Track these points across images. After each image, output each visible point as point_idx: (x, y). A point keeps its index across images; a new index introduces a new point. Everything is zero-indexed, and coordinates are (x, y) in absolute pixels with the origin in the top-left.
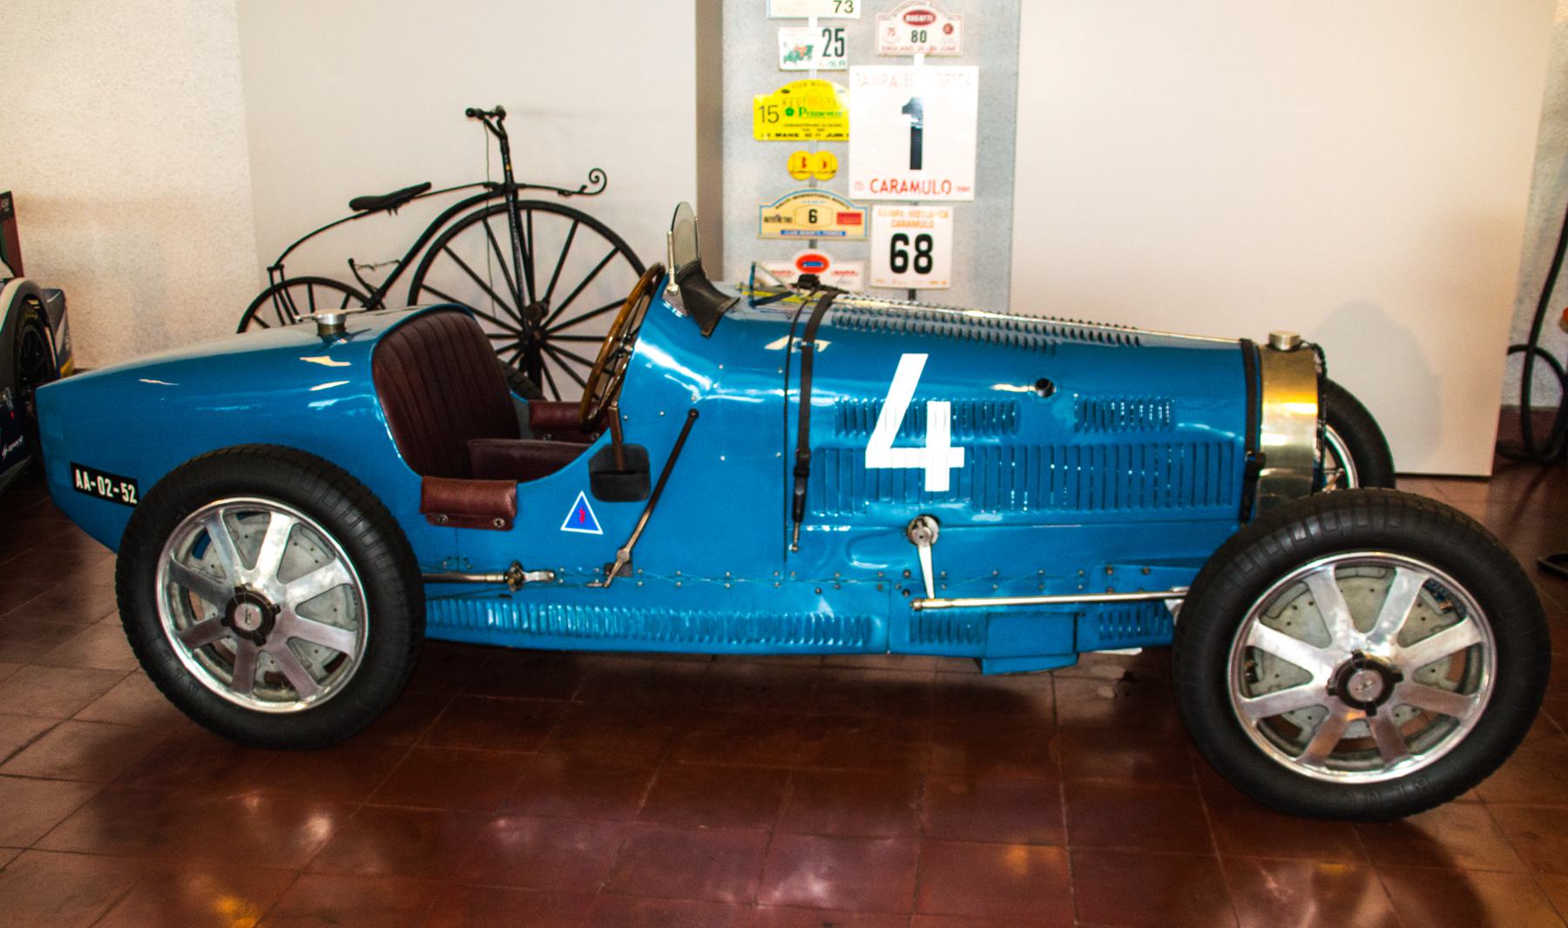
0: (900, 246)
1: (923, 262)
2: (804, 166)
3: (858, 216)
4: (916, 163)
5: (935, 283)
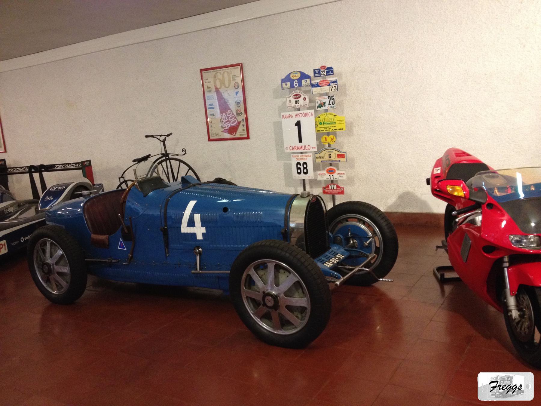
0: (299, 166)
1: (305, 171)
2: (326, 140)
3: (344, 155)
4: (300, 141)
5: (310, 177)
